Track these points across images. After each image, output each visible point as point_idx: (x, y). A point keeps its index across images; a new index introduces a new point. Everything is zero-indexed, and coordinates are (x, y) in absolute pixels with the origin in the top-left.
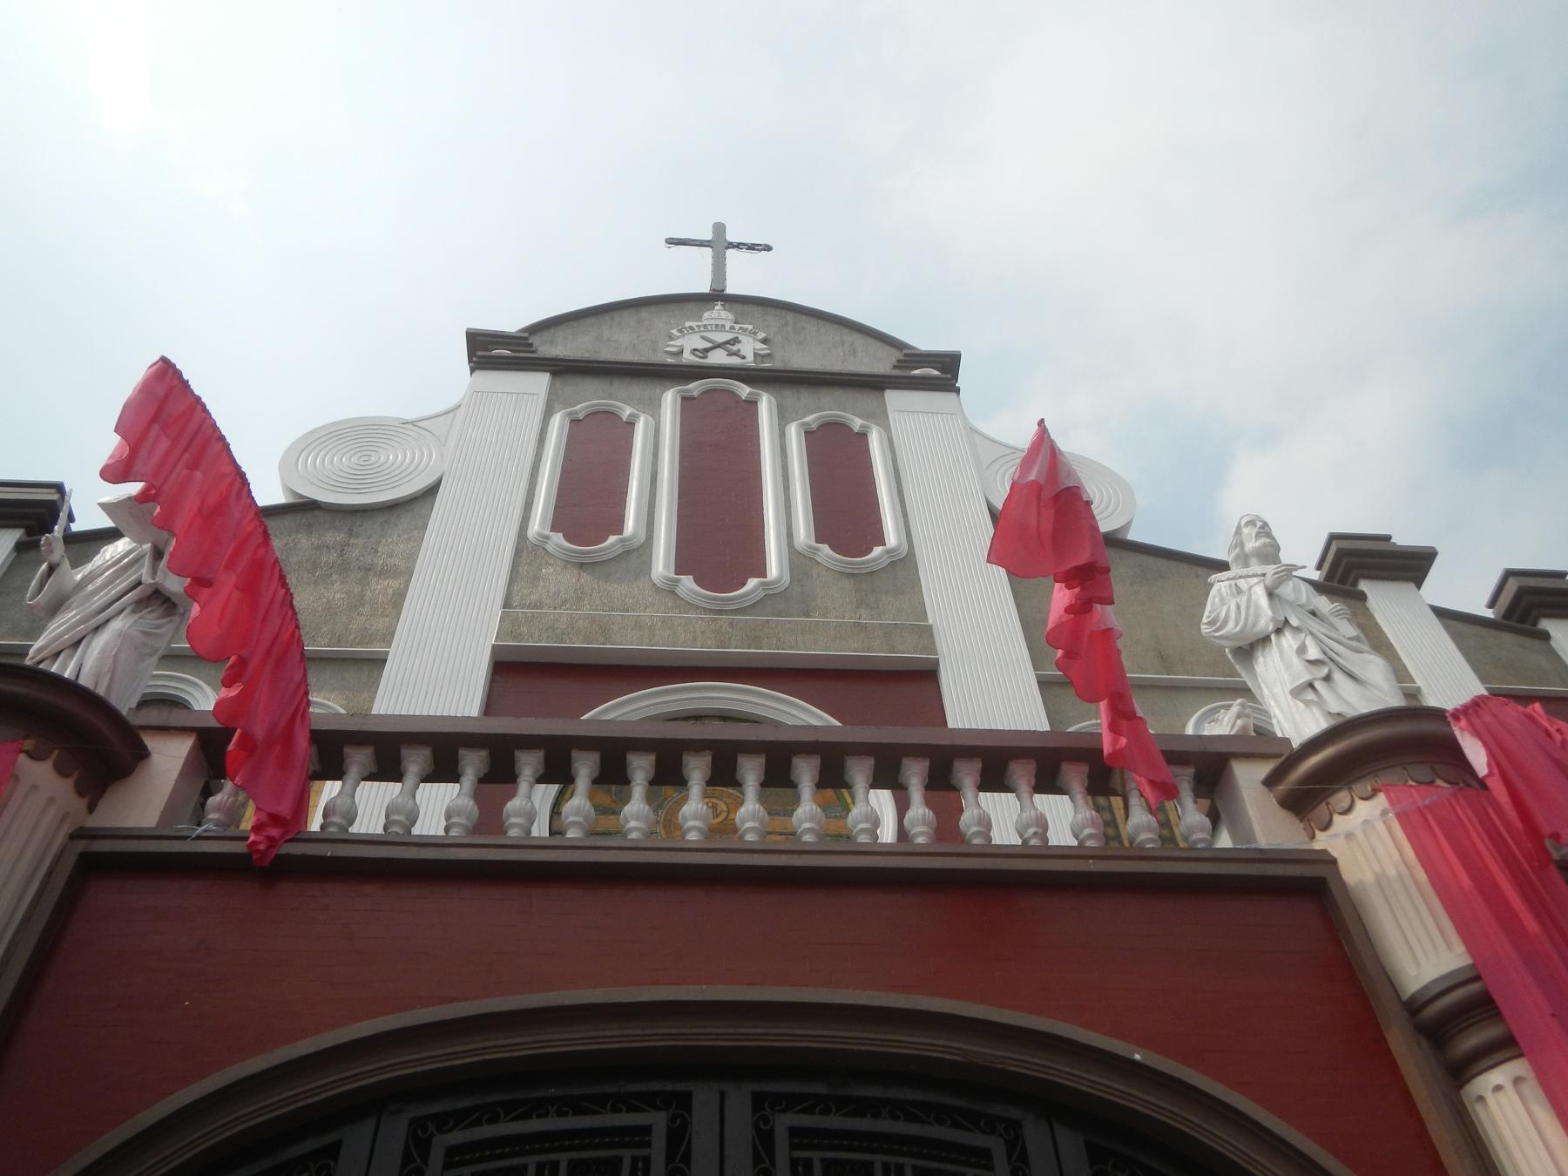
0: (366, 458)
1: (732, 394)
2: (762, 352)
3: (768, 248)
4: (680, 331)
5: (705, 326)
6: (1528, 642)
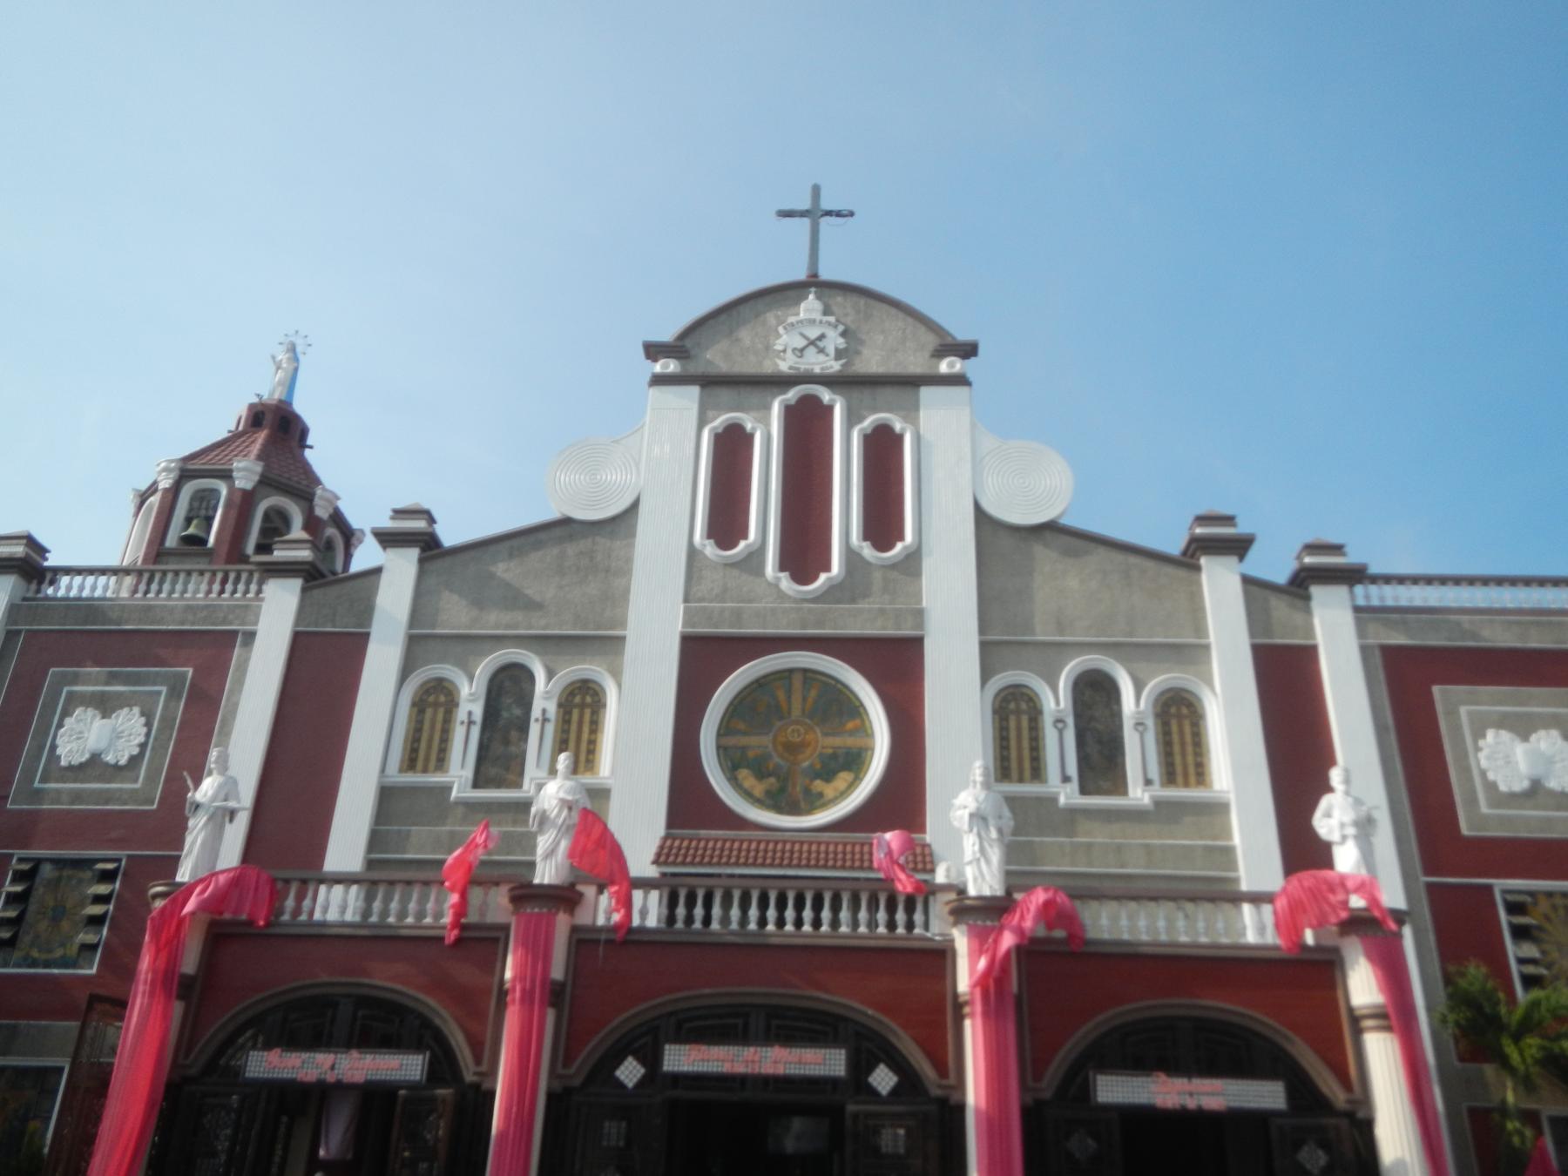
2: (841, 347)
3: (851, 214)
4: (785, 328)
5: (801, 322)
6: (1299, 603)
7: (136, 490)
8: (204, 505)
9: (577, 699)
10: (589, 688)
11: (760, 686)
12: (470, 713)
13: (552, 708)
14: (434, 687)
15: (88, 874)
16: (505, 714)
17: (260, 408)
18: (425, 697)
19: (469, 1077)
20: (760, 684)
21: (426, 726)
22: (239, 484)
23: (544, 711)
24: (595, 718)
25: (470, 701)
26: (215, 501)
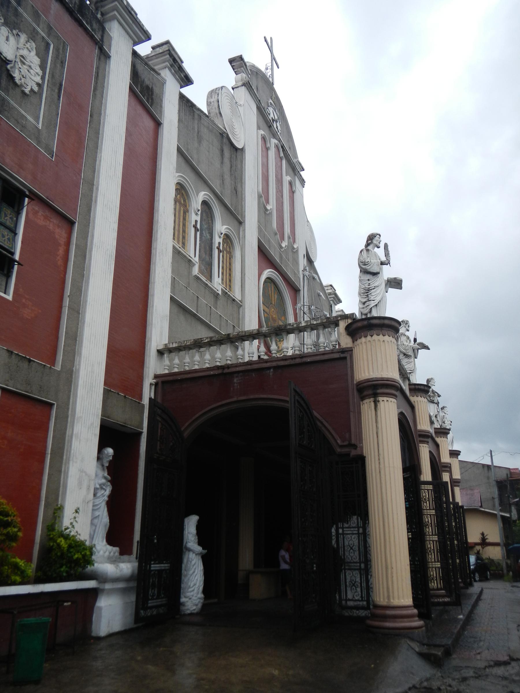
3: (278, 68)
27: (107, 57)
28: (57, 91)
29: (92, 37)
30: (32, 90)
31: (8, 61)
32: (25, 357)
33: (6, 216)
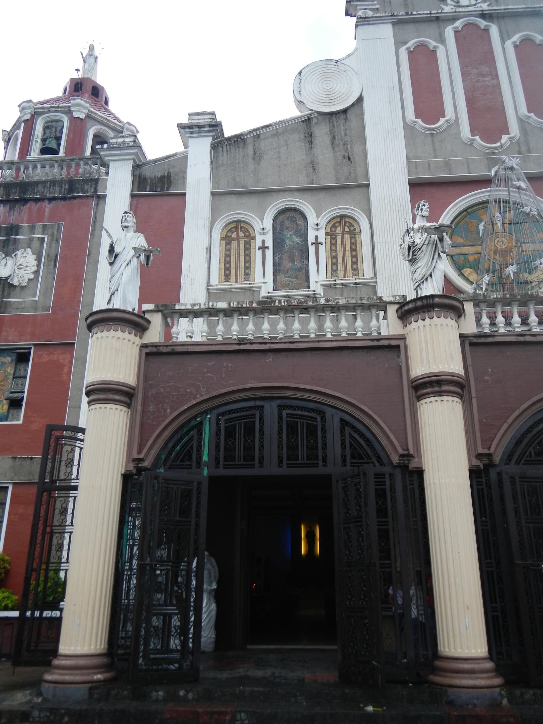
0: (328, 85)
1: (477, 26)
7: (3, 131)
8: (54, 129)
9: (339, 229)
10: (345, 222)
11: (469, 214)
12: (263, 242)
13: (321, 235)
14: (235, 227)
15: (8, 359)
16: (287, 241)
17: (79, 81)
18: (229, 234)
19: (395, 459)
20: (467, 212)
21: (233, 252)
22: (76, 115)
23: (316, 237)
24: (353, 241)
25: (263, 234)
26: (60, 128)
27: (104, 197)
28: (53, 263)
29: (87, 196)
30: (30, 280)
31: (8, 277)
32: (28, 457)
33: (20, 370)
